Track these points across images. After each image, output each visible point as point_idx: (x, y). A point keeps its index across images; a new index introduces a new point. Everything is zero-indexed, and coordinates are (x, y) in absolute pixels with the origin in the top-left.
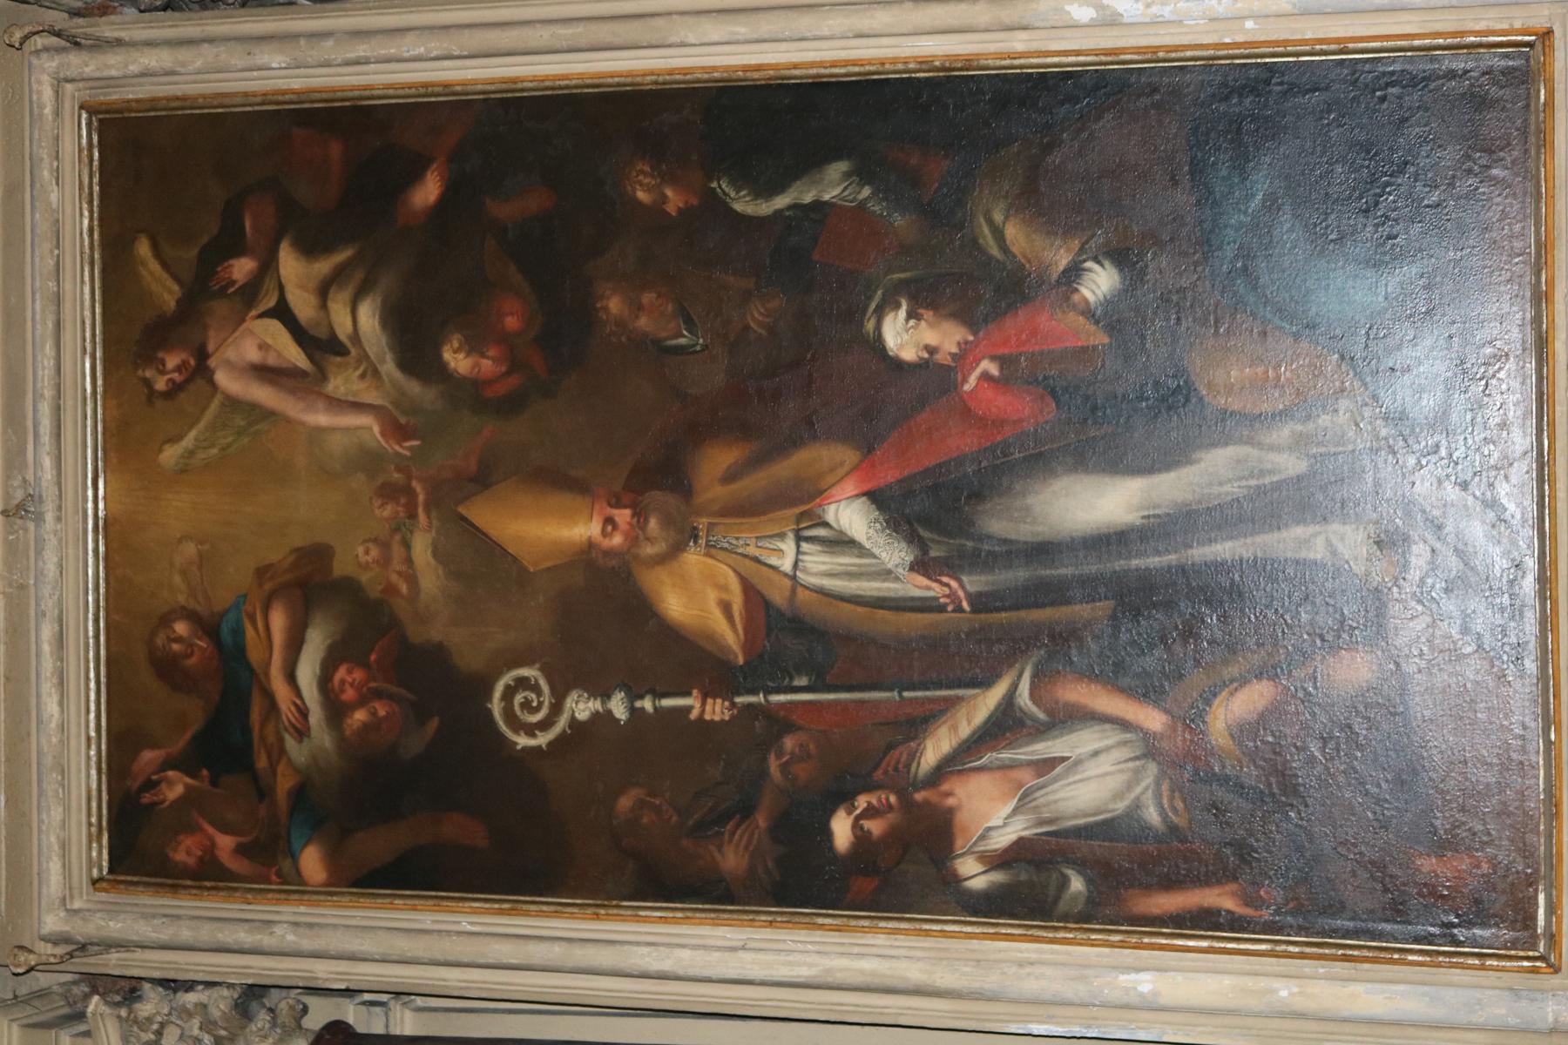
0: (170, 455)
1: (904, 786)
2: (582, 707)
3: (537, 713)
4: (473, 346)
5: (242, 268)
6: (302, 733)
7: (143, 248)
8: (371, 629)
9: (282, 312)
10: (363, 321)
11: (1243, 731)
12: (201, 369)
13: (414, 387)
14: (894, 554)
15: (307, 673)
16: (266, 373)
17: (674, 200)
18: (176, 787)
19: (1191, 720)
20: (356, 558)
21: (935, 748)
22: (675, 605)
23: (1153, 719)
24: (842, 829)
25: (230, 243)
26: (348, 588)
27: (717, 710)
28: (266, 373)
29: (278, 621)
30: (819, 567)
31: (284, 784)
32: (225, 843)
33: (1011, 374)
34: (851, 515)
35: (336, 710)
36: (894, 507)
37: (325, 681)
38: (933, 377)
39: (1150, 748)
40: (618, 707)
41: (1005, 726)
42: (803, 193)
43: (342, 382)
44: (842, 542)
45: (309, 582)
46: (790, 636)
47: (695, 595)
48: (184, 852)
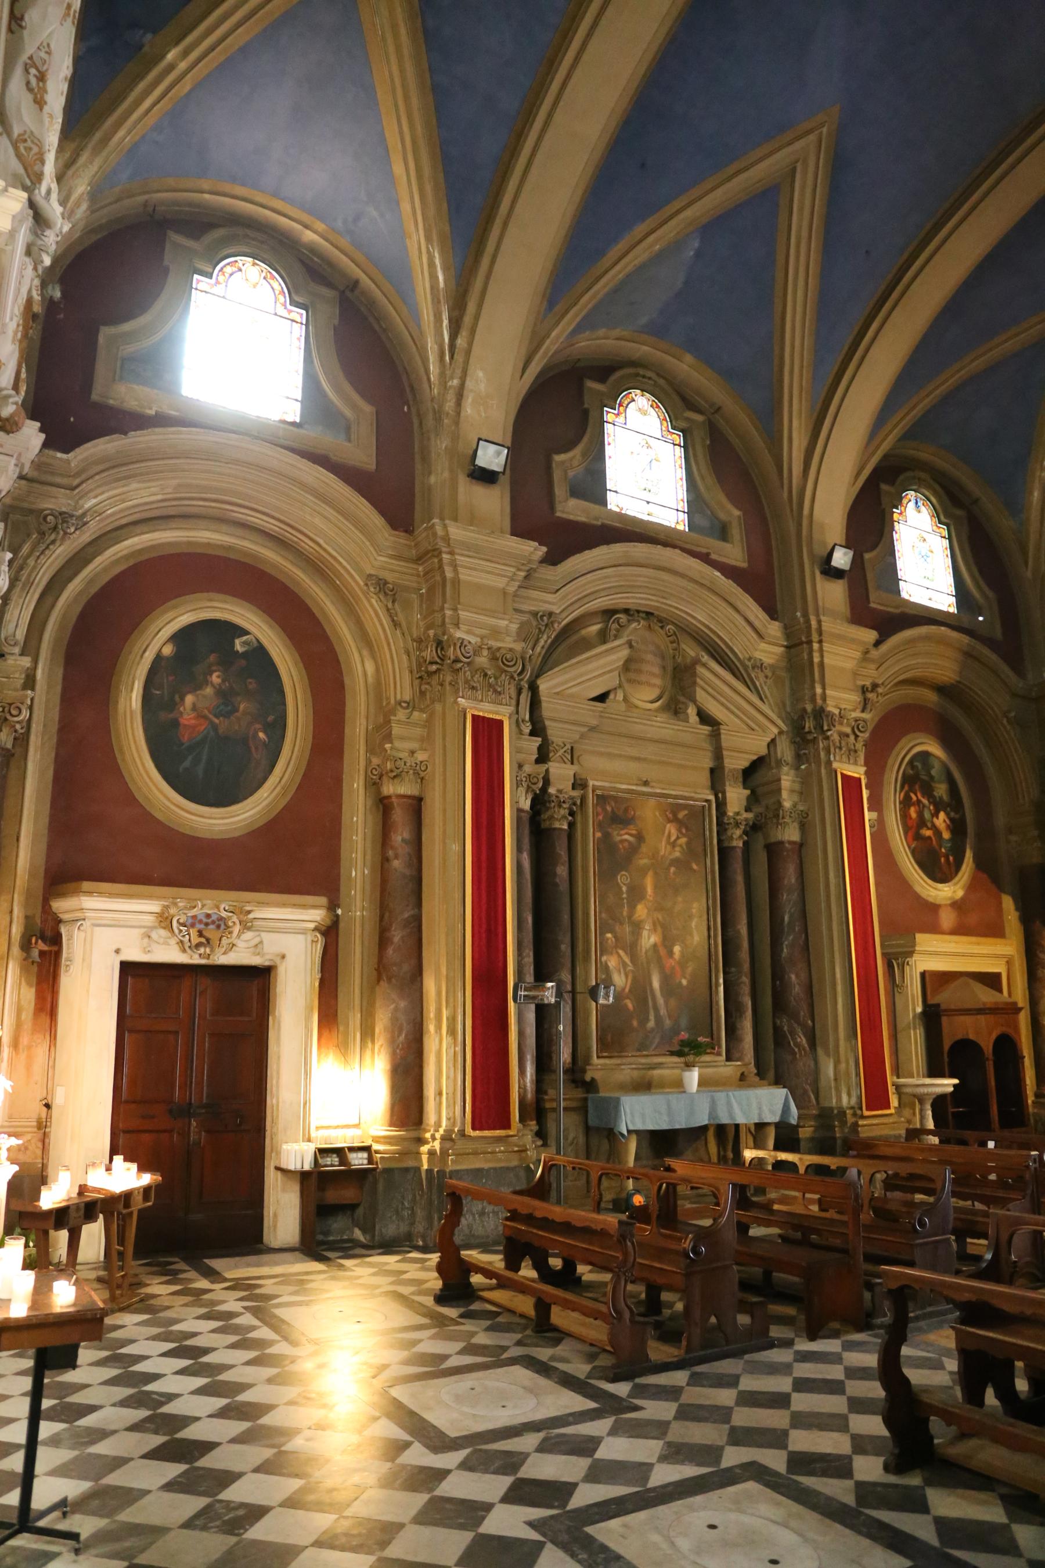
0: (657, 814)
1: (616, 947)
2: (624, 889)
3: (623, 879)
4: (674, 873)
5: (684, 831)
6: (618, 835)
7: (686, 812)
8: (634, 850)
9: (678, 838)
10: (677, 854)
11: (626, 1005)
12: (669, 821)
13: (668, 862)
14: (648, 946)
15: (626, 837)
16: (670, 833)
17: (694, 911)
18: (609, 809)
19: (628, 998)
20: (644, 849)
21: (621, 952)
22: (640, 907)
23: (627, 990)
24: (609, 935)
25: (687, 829)
26: (639, 846)
27: (625, 914)
28: (670, 833)
29: (634, 832)
30: (645, 933)
31: (610, 830)
32: (601, 818)
33: (673, 968)
34: (653, 939)
35: (622, 841)
36: (655, 945)
37: (626, 840)
38: (671, 953)
39: (624, 989)
40: (625, 896)
41: (625, 965)
42: (695, 933)
43: (669, 847)
44: (649, 938)
45: (640, 838)
46: (637, 927)
47: (641, 911)
48: (599, 809)
